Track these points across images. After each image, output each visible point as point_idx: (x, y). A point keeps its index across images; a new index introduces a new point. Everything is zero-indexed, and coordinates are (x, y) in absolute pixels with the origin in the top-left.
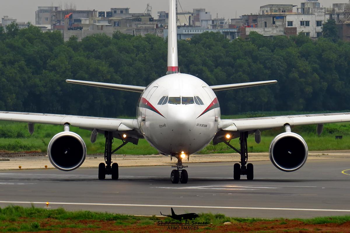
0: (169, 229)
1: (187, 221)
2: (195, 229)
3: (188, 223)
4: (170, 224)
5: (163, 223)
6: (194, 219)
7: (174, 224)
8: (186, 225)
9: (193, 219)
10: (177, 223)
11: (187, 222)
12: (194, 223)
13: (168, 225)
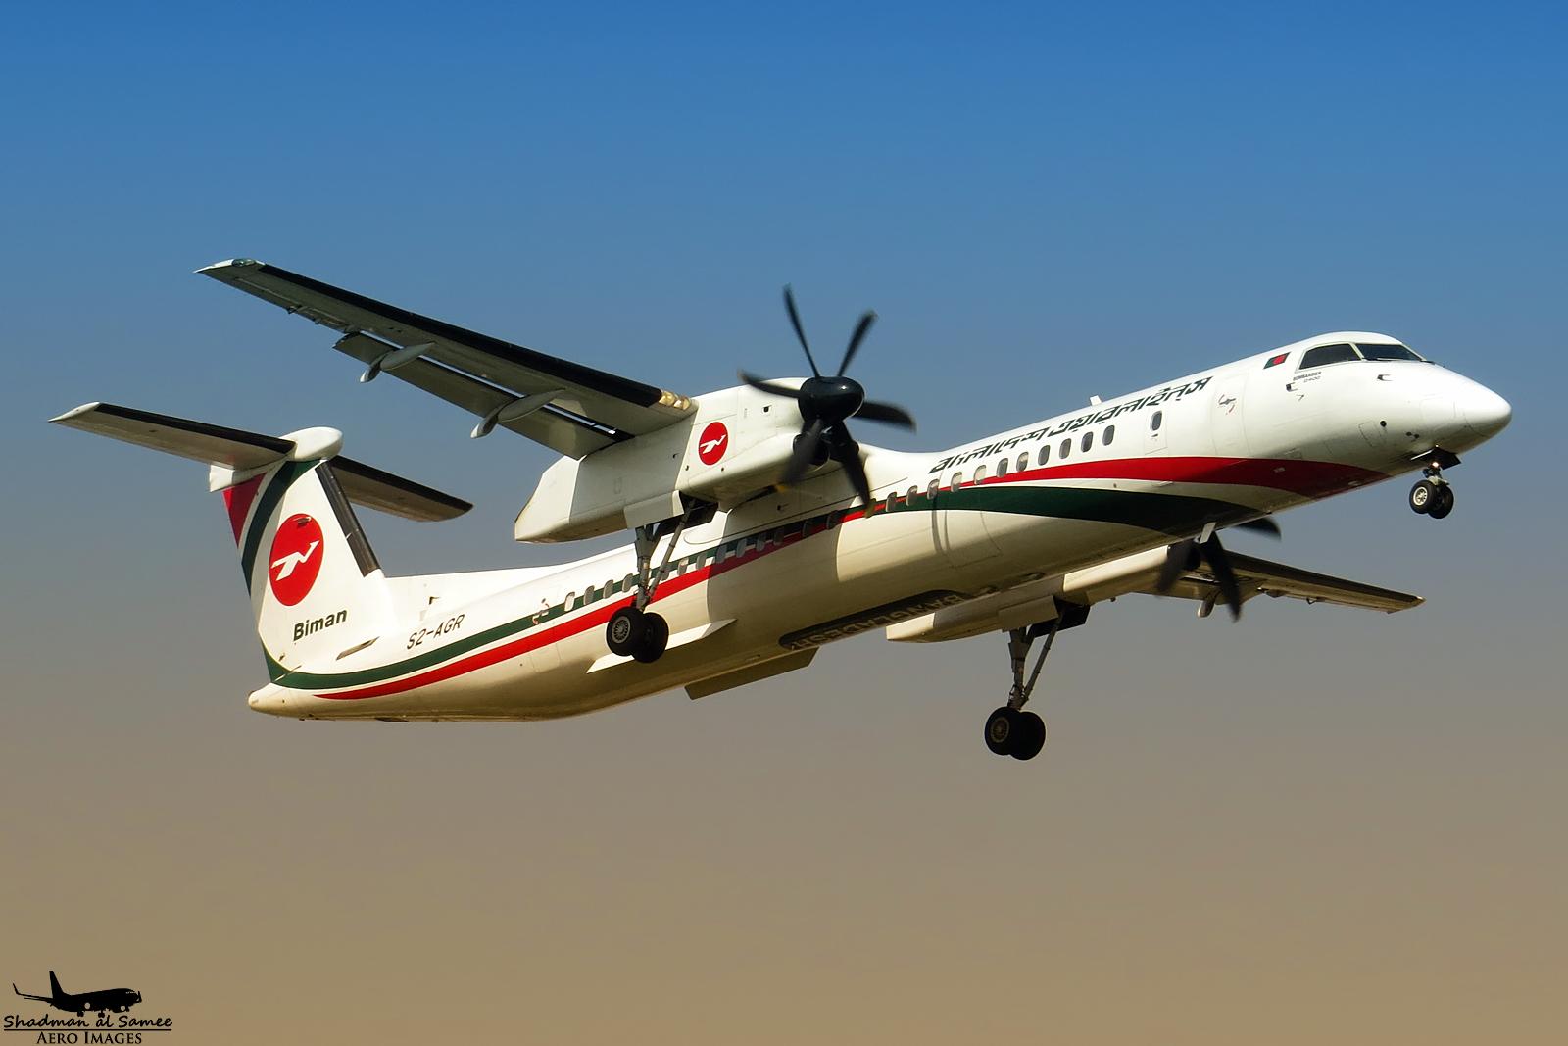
0: (42, 1041)
1: (101, 1015)
2: (131, 1041)
3: (107, 1022)
4: (45, 1027)
5: (22, 1021)
6: (127, 1010)
7: (58, 1025)
8: (100, 1028)
9: (123, 1008)
10: (72, 1022)
11: (104, 1020)
12: (128, 1021)
13: (38, 1027)
